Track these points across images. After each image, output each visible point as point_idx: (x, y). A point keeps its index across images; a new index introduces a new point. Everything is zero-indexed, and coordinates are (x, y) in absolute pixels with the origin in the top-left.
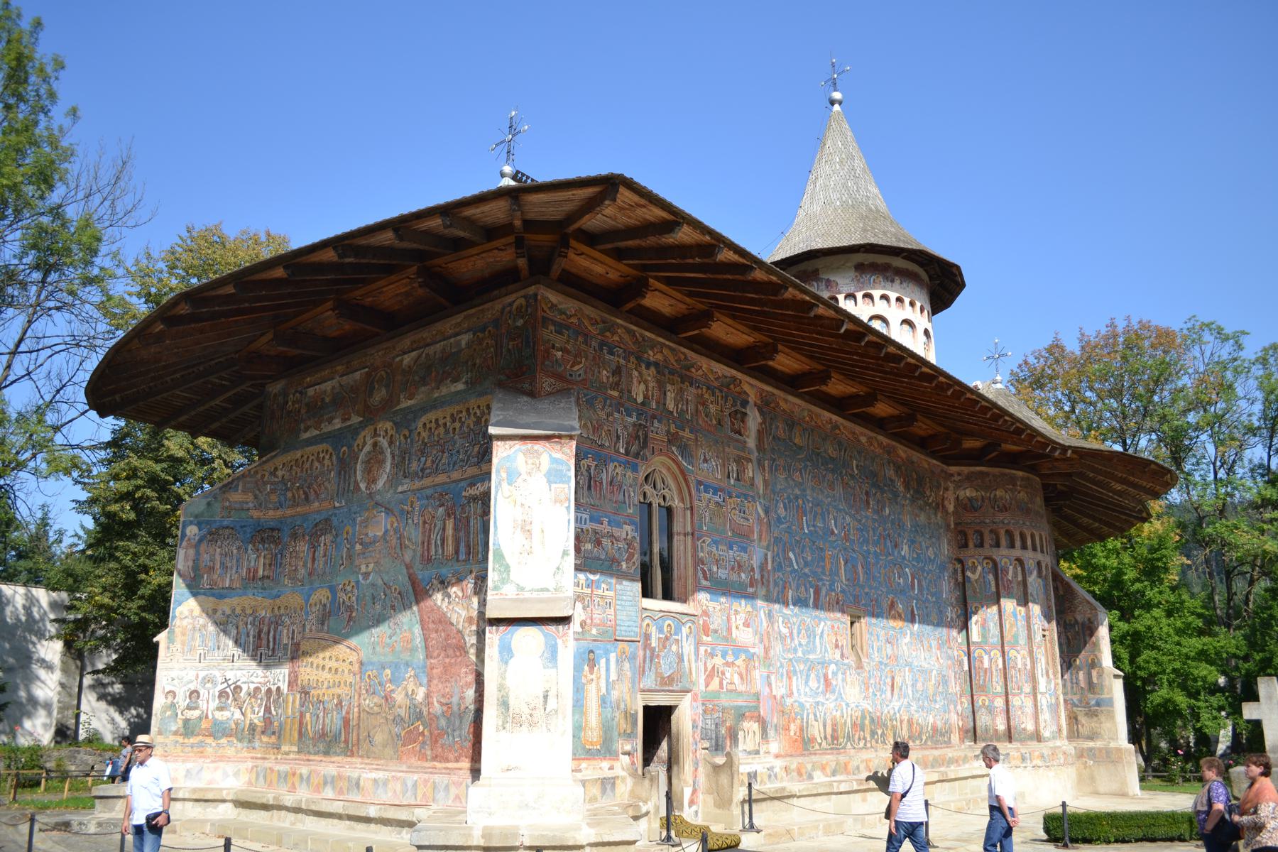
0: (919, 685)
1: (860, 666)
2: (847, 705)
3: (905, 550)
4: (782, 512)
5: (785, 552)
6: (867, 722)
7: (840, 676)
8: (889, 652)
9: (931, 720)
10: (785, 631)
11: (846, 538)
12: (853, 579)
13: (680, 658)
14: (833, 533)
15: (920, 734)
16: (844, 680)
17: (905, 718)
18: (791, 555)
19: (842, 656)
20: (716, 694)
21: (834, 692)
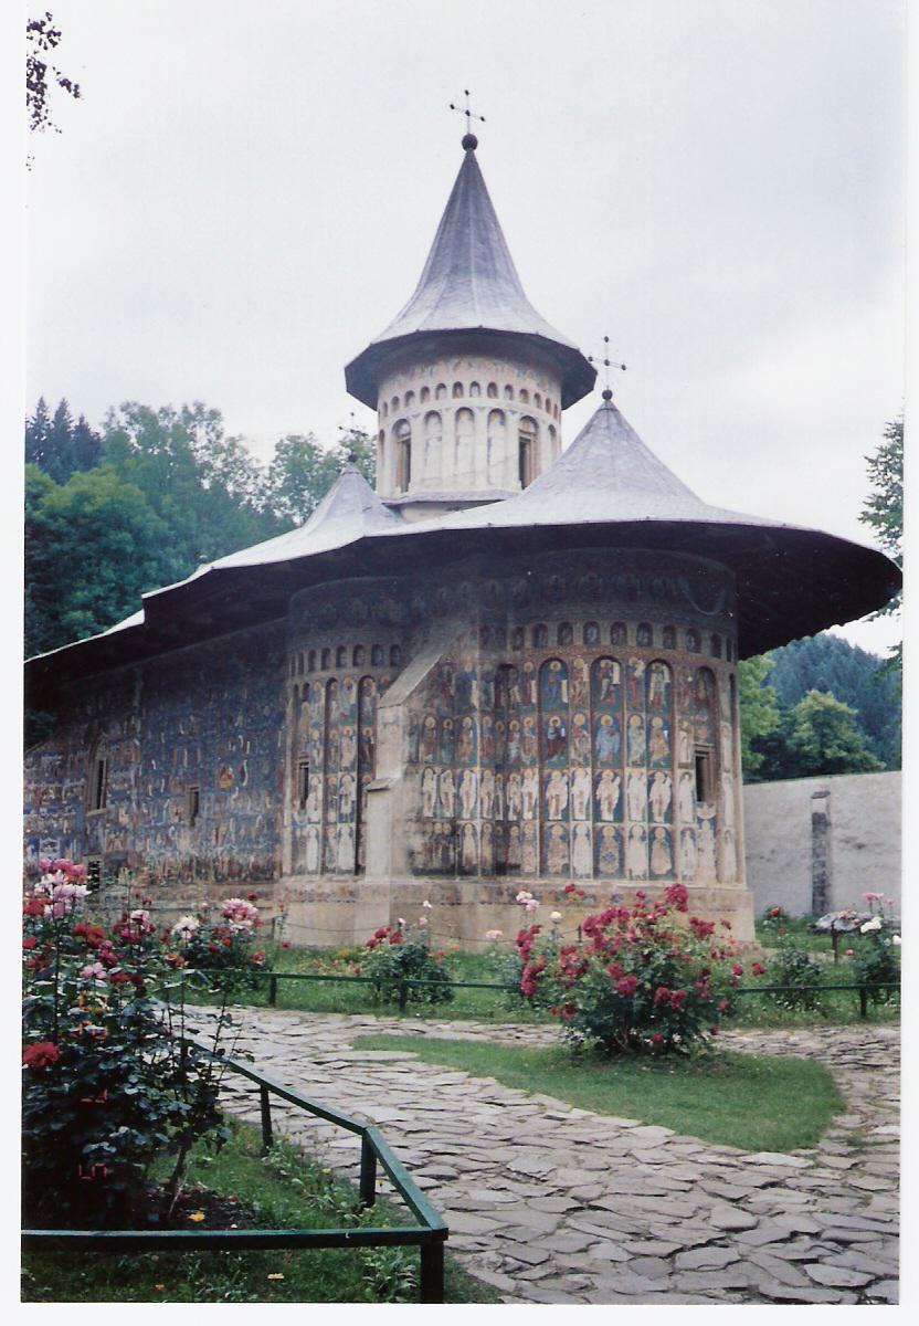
0: (242, 832)
1: (193, 824)
2: (180, 853)
3: (240, 718)
4: (150, 736)
5: (150, 760)
6: (194, 863)
7: (176, 834)
8: (217, 809)
9: (252, 859)
10: (146, 811)
11: (191, 734)
12: (192, 762)
13: (97, 837)
14: (180, 734)
15: (240, 871)
16: (179, 836)
17: (227, 859)
18: (153, 762)
19: (180, 819)
20: (110, 854)
21: (171, 846)
